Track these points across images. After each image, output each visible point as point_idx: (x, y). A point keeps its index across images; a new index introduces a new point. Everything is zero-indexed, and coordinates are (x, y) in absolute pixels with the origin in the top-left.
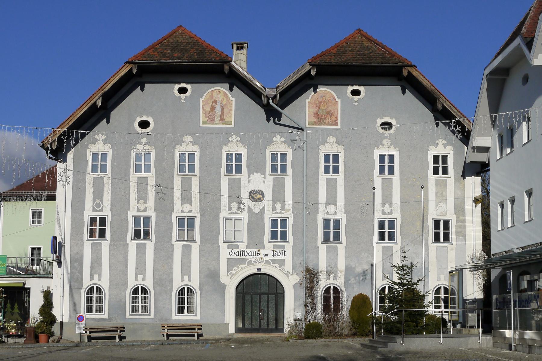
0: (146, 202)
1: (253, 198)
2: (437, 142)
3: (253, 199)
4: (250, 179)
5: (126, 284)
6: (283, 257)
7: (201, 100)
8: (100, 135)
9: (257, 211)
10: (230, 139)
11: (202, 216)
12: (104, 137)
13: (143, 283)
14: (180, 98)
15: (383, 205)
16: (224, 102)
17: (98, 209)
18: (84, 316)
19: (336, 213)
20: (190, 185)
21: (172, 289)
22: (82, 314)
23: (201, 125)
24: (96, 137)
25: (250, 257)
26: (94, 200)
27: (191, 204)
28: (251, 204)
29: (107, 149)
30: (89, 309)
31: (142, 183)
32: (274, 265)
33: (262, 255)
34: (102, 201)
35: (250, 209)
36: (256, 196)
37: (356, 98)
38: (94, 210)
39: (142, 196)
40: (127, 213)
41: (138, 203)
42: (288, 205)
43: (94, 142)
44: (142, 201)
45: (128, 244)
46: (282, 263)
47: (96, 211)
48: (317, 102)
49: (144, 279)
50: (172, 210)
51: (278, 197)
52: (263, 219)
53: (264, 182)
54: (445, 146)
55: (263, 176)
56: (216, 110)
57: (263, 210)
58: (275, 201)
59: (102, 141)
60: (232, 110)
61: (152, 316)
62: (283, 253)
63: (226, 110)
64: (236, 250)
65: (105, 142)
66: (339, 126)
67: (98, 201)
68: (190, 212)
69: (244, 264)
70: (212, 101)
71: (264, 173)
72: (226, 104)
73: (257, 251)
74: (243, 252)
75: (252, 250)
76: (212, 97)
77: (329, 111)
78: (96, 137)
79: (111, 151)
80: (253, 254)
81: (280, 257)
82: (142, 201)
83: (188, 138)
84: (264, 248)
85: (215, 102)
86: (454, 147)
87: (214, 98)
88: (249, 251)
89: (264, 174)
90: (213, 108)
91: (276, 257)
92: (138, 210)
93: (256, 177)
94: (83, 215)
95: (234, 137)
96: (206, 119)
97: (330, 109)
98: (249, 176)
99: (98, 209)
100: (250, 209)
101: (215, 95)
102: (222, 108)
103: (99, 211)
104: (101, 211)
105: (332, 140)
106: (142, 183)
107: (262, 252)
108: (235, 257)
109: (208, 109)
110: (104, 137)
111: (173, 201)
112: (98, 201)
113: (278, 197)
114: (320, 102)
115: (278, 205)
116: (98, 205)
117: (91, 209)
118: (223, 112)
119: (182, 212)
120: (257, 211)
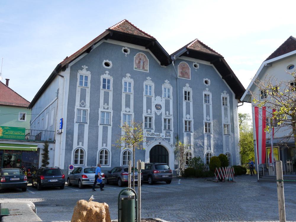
0: (108, 105)
1: (157, 108)
2: (224, 92)
3: (157, 109)
4: (156, 98)
5: (97, 148)
6: (170, 138)
7: (135, 57)
8: (85, 66)
9: (158, 114)
10: (147, 78)
11: (135, 114)
12: (87, 67)
13: (106, 148)
14: (125, 55)
15: (207, 117)
16: (144, 60)
17: (83, 106)
18: (73, 166)
19: (190, 118)
21: (120, 152)
22: (72, 164)
24: (83, 66)
25: (156, 137)
26: (81, 101)
27: (130, 108)
28: (156, 111)
29: (88, 74)
30: (76, 162)
31: (106, 95)
32: (166, 141)
33: (161, 136)
34: (85, 101)
35: (156, 114)
36: (158, 107)
37: (196, 68)
38: (81, 106)
39: (106, 101)
40: (98, 110)
41: (104, 104)
42: (171, 113)
43: (82, 69)
44: (106, 104)
45: (98, 127)
46: (169, 140)
47: (82, 107)
48: (182, 67)
49: (106, 146)
50: (121, 110)
51: (167, 109)
52: (161, 119)
53: (162, 101)
54: (227, 93)
55: (161, 98)
56: (141, 63)
57: (161, 114)
58: (166, 110)
59: (86, 69)
60: (148, 65)
61: (110, 166)
62: (170, 136)
63: (145, 64)
64: (150, 133)
65: (87, 70)
66: (190, 79)
67: (83, 101)
68: (129, 112)
69: (153, 140)
70: (139, 58)
71: (161, 97)
72: (145, 61)
73: (159, 134)
74: (153, 134)
75: (157, 133)
76: (139, 56)
77: (186, 72)
78: (83, 66)
79: (90, 75)
80: (157, 135)
81: (168, 138)
82: (106, 104)
83: (128, 75)
84: (162, 133)
85: (140, 59)
86: (229, 94)
87: (140, 57)
88: (155, 133)
89: (162, 97)
90: (139, 62)
91: (167, 137)
92: (104, 108)
93: (158, 98)
94: (74, 108)
95: (149, 77)
97: (187, 71)
98: (155, 97)
99: (83, 106)
100: (156, 114)
101: (141, 56)
102: (144, 63)
103: (83, 107)
104: (84, 107)
105: (187, 85)
106: (106, 95)
107: (161, 135)
108: (149, 136)
109: (137, 62)
110: (87, 67)
111: (121, 105)
112: (83, 101)
113: (167, 109)
114: (183, 67)
115: (167, 112)
116: (83, 104)
117: (79, 105)
118: (144, 64)
119: (126, 111)
120: (158, 114)
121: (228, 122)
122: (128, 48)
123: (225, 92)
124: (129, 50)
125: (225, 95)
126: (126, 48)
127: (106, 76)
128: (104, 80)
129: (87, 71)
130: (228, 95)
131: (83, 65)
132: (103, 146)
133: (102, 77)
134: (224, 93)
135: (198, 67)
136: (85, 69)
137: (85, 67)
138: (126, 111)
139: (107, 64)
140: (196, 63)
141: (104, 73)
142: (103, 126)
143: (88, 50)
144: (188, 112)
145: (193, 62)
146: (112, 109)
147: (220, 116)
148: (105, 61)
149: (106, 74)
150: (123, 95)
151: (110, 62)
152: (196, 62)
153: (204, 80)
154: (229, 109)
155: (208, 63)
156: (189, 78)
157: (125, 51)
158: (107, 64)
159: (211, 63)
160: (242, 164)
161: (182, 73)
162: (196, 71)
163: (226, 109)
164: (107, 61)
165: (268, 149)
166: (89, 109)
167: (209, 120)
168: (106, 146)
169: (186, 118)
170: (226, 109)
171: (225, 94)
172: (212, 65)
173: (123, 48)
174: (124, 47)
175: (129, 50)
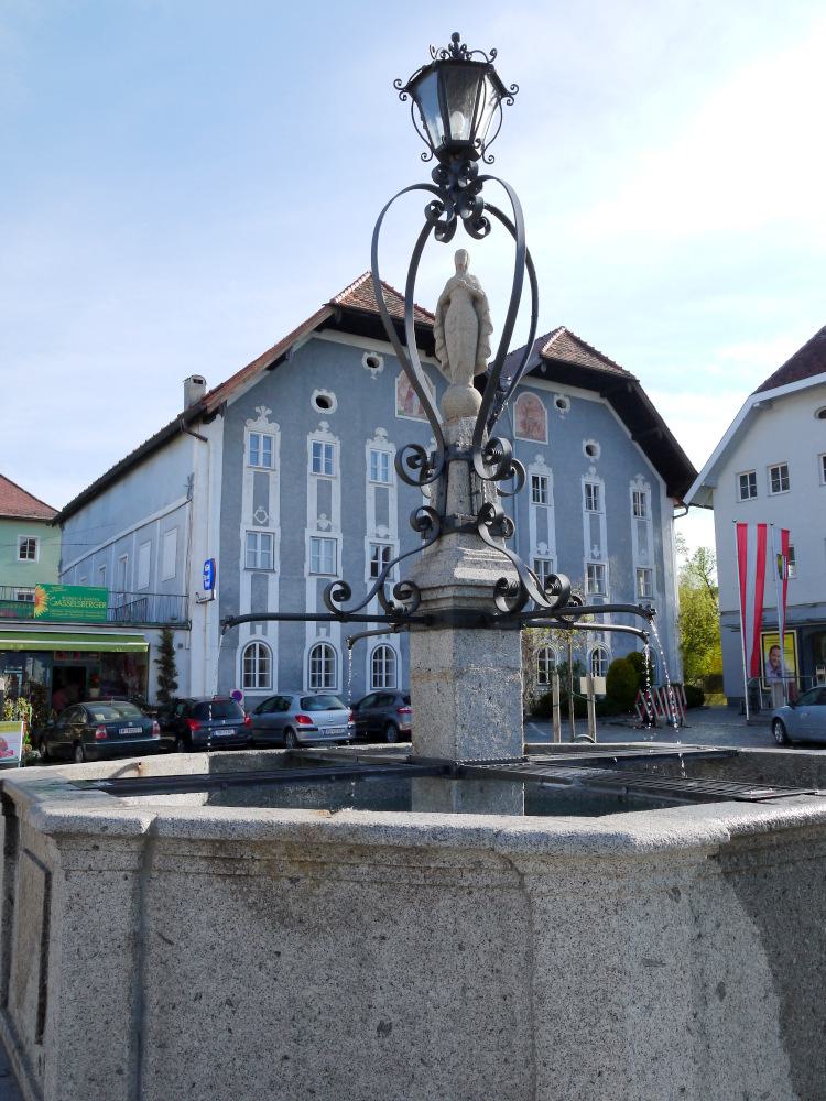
0: (329, 518)
5: (303, 642)
7: (397, 379)
8: (263, 408)
11: (402, 544)
13: (327, 640)
14: (370, 373)
15: (592, 548)
17: (261, 522)
18: (242, 691)
20: (386, 499)
21: (366, 650)
22: (238, 688)
23: (397, 415)
24: (257, 410)
26: (255, 509)
27: (387, 525)
29: (273, 430)
30: (248, 681)
31: (324, 488)
34: (267, 509)
38: (255, 523)
39: (324, 508)
40: (303, 532)
41: (318, 517)
43: (255, 417)
44: (323, 516)
45: (305, 580)
47: (259, 525)
49: (328, 634)
54: (644, 481)
59: (267, 416)
65: (271, 419)
66: (547, 443)
67: (261, 509)
68: (387, 537)
78: (257, 410)
82: (323, 516)
83: (381, 432)
92: (319, 529)
96: (403, 409)
104: (266, 525)
105: (540, 458)
106: (324, 488)
110: (269, 411)
112: (261, 509)
116: (261, 516)
117: (251, 521)
119: (377, 536)
121: (647, 563)
122: (379, 354)
123: (640, 477)
124: (381, 360)
125: (639, 485)
126: (373, 355)
127: (322, 436)
128: (317, 447)
129: (270, 422)
130: (648, 485)
131: (259, 405)
132: (318, 634)
133: (311, 439)
134: (636, 481)
135: (568, 409)
136: (263, 416)
137: (264, 411)
138: (377, 536)
139: (323, 403)
140: (561, 397)
141: (315, 427)
142: (318, 580)
143: (279, 361)
144: (543, 537)
145: (554, 393)
146: (339, 531)
147: (629, 544)
148: (317, 393)
149: (320, 429)
150: (584, 517)
151: (332, 397)
152: (562, 392)
153: (585, 444)
154: (650, 525)
155: (592, 396)
156: (544, 440)
157: (371, 363)
158: (323, 403)
159: (602, 396)
160: (686, 678)
161: (524, 424)
162: (562, 417)
163: (642, 526)
164: (324, 393)
165: (766, 638)
166: (278, 531)
167: (599, 558)
168: (328, 634)
169: (539, 552)
170: (642, 526)
171: (640, 482)
172: (605, 401)
173: (366, 356)
174: (369, 352)
175: (381, 360)
